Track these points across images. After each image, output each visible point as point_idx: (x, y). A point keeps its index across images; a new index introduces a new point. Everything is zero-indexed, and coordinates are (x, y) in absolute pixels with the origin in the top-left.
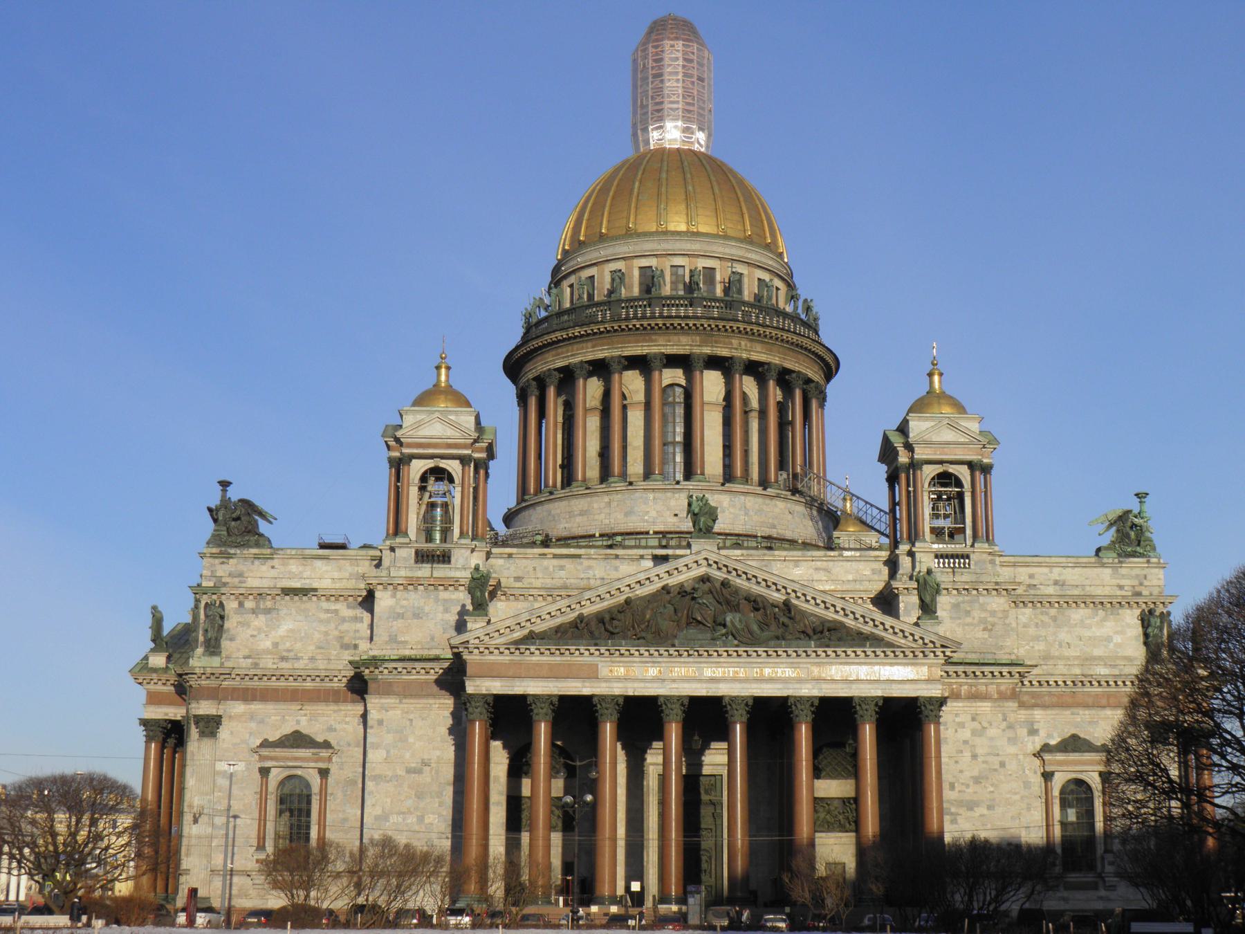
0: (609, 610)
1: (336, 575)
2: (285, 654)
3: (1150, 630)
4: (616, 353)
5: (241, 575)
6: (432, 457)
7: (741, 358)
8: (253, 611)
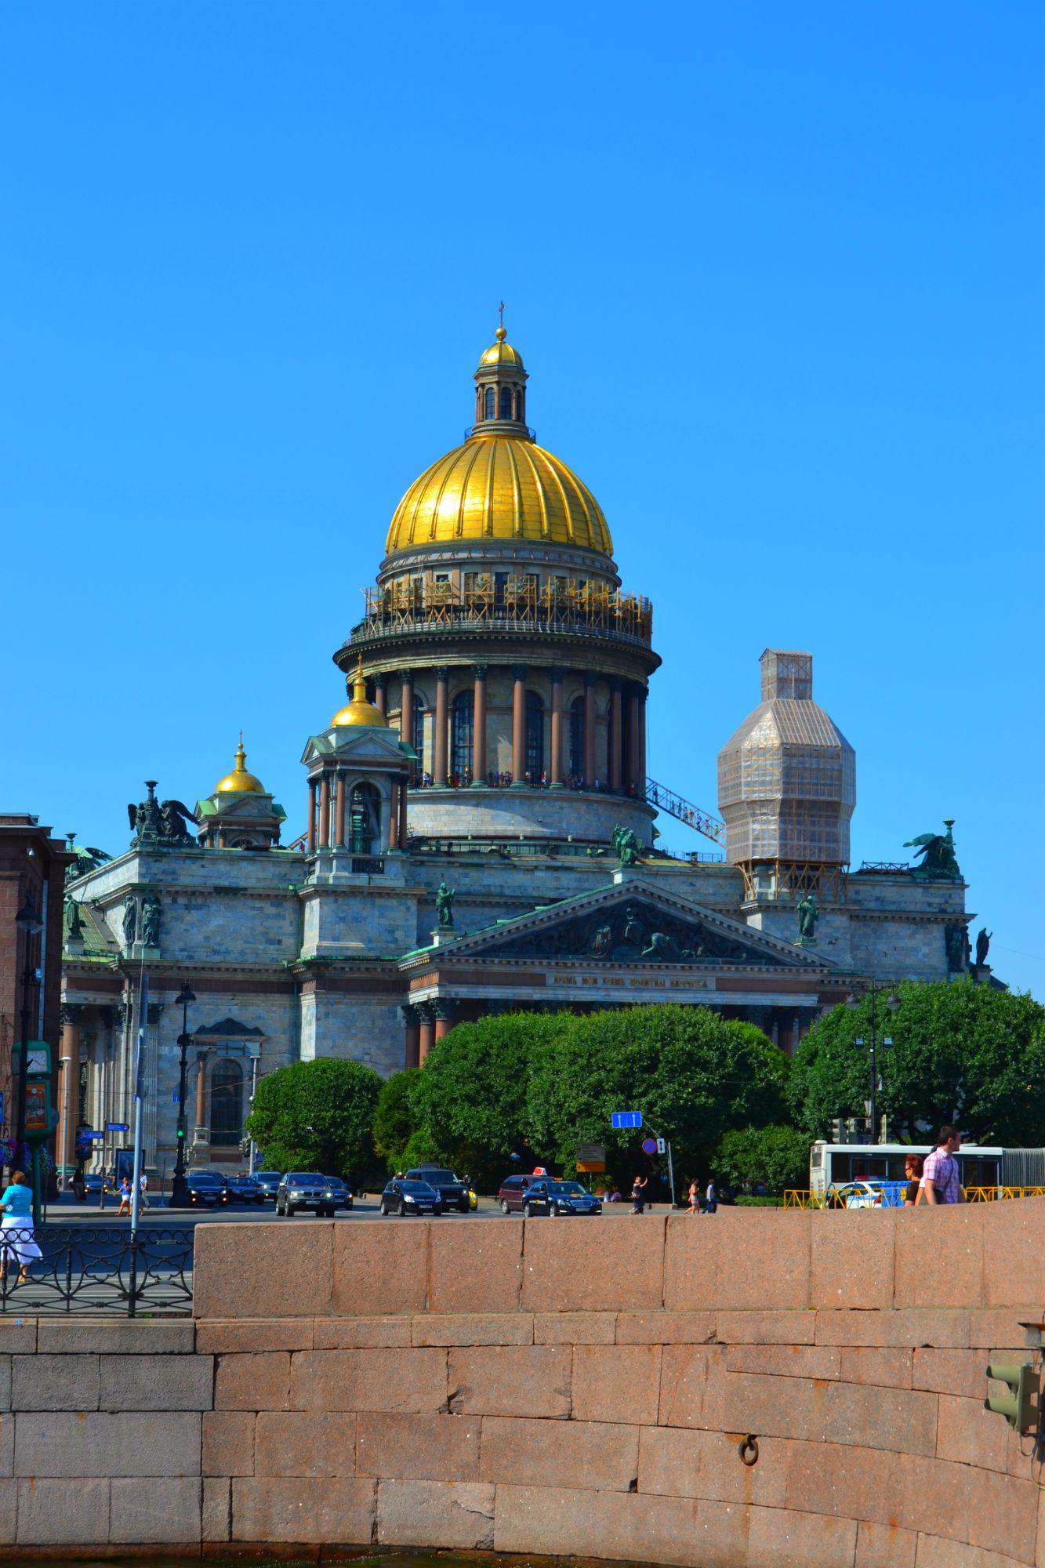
1: (261, 875)
2: (216, 947)
4: (484, 661)
5: (174, 873)
6: (364, 773)
7: (594, 671)
8: (187, 907)
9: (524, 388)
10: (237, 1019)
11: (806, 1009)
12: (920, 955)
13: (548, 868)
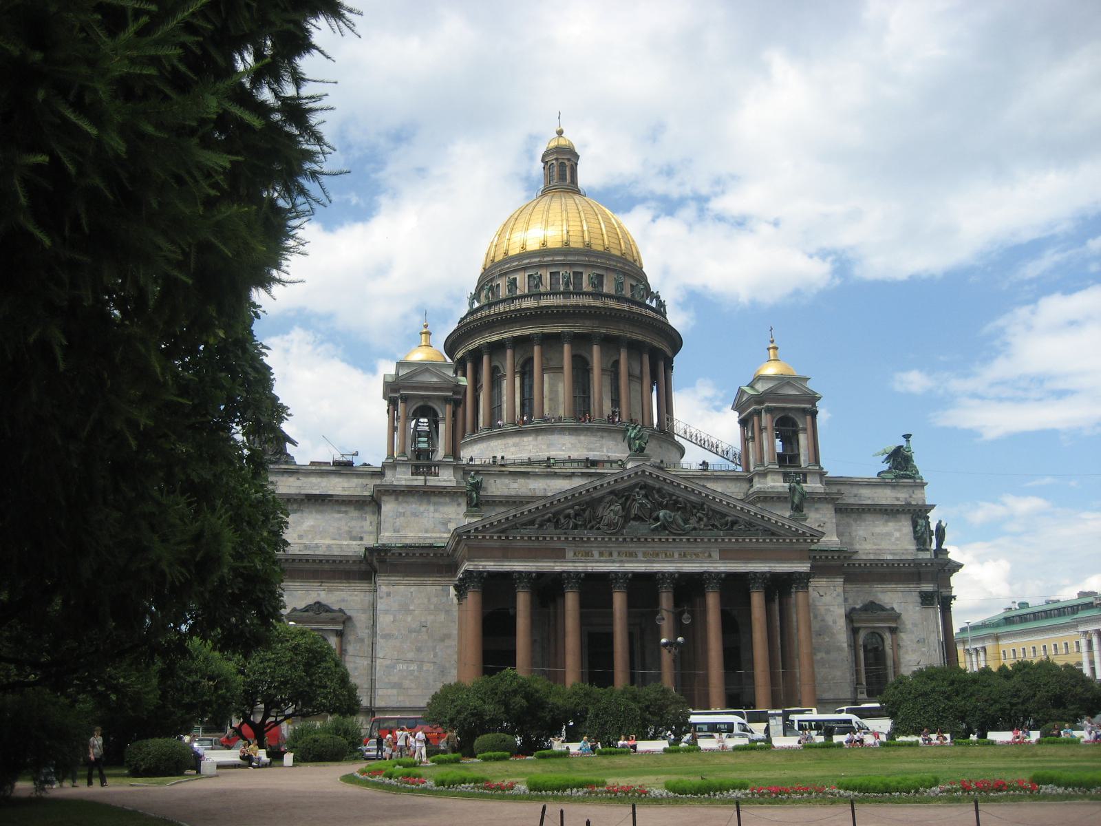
0: (572, 507)
1: (346, 485)
3: (919, 528)
4: (538, 331)
6: (422, 397)
9: (576, 164)
10: (324, 602)
11: (800, 573)
12: (893, 539)
13: (583, 475)
